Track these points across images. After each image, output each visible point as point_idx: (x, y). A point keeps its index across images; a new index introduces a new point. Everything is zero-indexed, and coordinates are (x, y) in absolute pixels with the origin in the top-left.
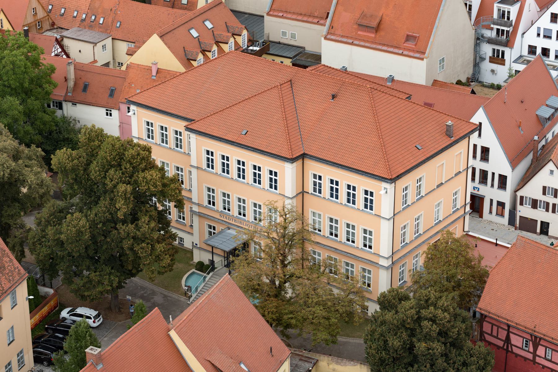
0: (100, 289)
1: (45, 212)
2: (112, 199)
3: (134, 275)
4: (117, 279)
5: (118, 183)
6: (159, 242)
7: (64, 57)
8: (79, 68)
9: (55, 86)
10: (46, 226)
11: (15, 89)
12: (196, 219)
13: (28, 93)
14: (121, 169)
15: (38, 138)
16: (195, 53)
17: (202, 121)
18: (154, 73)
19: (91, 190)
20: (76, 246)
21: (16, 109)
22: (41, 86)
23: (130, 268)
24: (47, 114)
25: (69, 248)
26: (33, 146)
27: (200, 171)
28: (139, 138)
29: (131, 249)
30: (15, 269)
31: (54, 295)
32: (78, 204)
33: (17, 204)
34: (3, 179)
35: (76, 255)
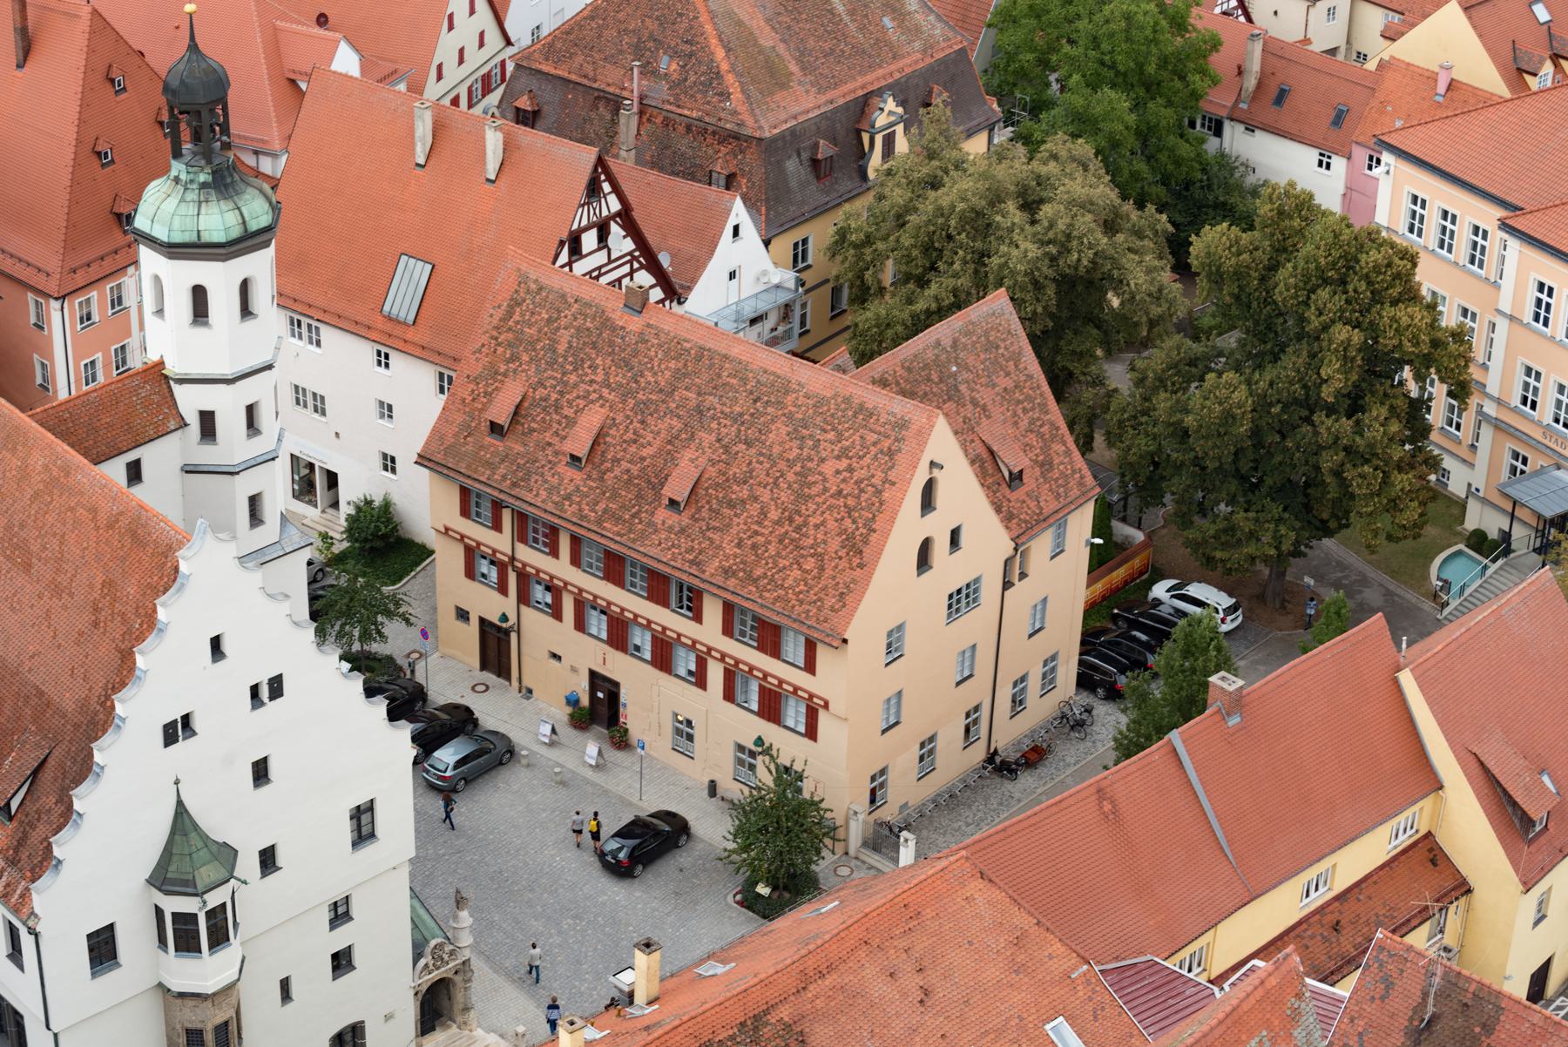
0: (1251, 549)
1: (1156, 358)
2: (1313, 356)
3: (1329, 533)
4: (1293, 535)
5: (1333, 322)
6: (1400, 470)
7: (1242, 19)
8: (1274, 49)
9: (1215, 82)
10: (1155, 390)
11: (1125, 75)
12: (1487, 433)
13: (1152, 87)
14: (1346, 292)
15: (1160, 190)
16: (1536, 59)
17: (1539, 214)
18: (1441, 89)
19: (1269, 328)
20: (1215, 446)
21: (1120, 119)
22: (1182, 78)
23: (1325, 516)
24: (1187, 141)
25: (1199, 446)
26: (1151, 208)
27: (1516, 327)
28: (1388, 229)
29: (1337, 474)
30: (1074, 472)
31: (1144, 546)
32: (1232, 353)
33: (1095, 331)
34: (1076, 269)
35: (1211, 465)
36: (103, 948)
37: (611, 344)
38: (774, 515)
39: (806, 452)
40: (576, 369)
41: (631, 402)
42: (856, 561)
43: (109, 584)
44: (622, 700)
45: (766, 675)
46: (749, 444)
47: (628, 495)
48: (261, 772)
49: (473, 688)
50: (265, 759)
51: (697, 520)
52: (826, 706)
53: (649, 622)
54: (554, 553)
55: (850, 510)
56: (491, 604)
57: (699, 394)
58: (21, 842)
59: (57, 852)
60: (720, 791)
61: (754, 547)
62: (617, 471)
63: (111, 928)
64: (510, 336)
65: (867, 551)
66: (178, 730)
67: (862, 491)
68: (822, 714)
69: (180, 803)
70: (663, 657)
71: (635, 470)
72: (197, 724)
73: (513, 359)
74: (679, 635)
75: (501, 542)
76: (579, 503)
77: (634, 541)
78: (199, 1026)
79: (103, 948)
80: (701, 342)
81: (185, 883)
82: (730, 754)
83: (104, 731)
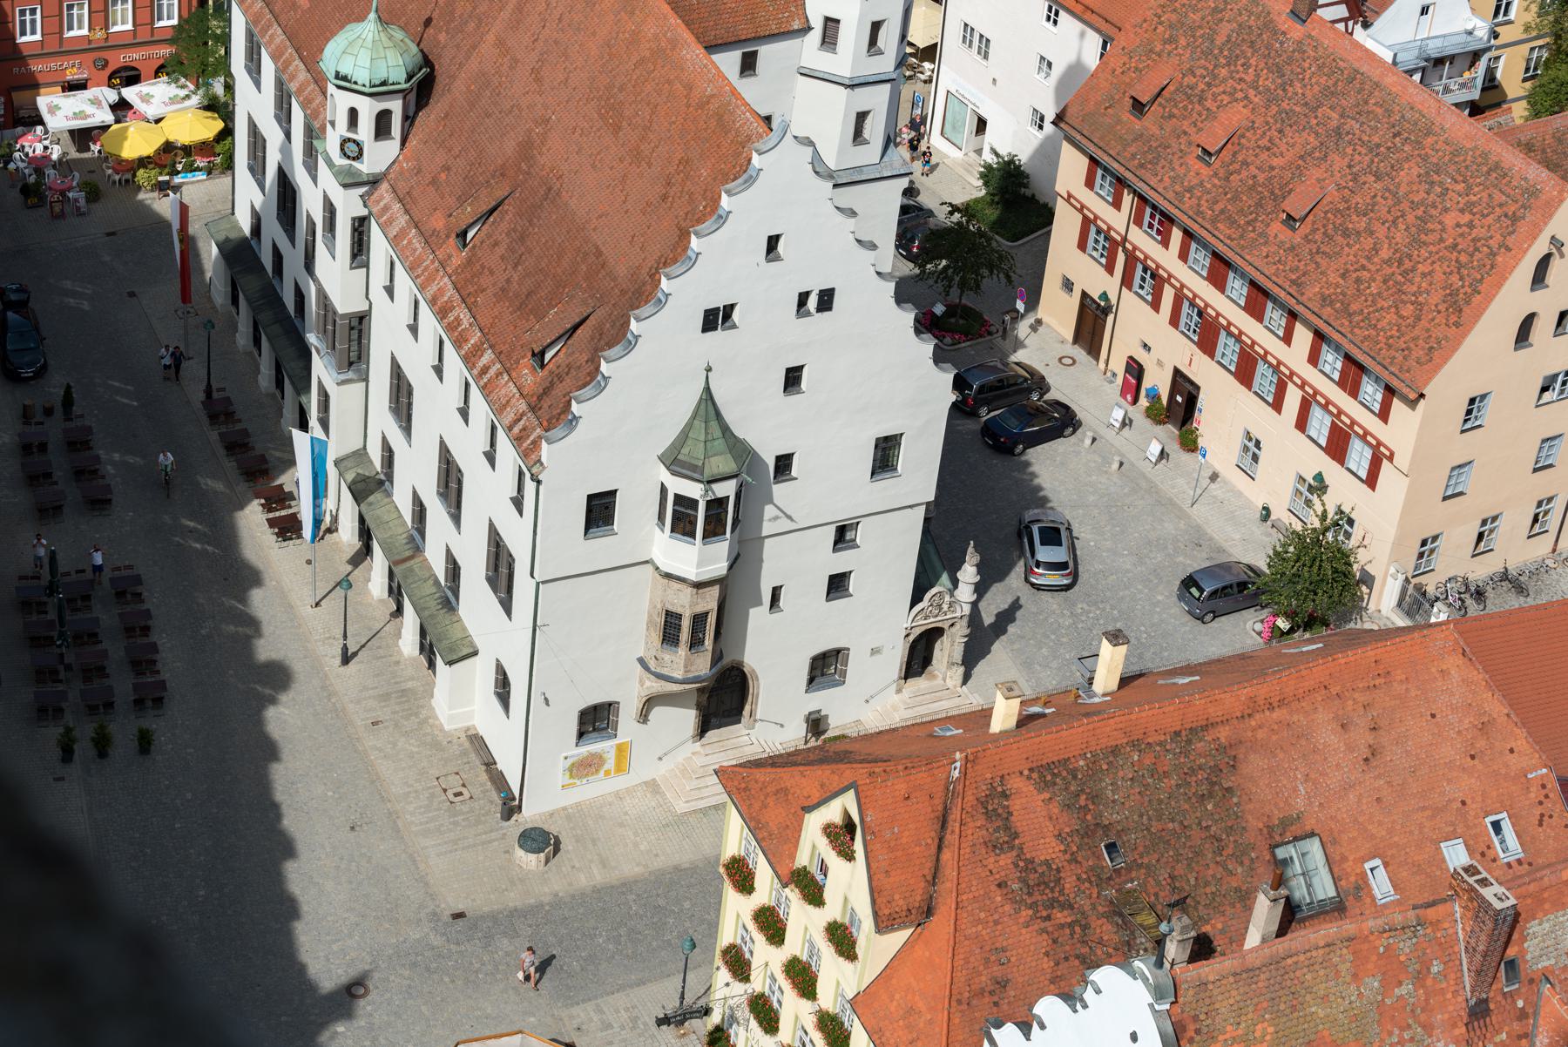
36: (600, 511)
37: (1269, 47)
38: (1385, 253)
39: (1432, 197)
40: (1229, 65)
41: (1275, 109)
42: (1453, 319)
43: (685, 162)
44: (1199, 405)
45: (1340, 412)
46: (1378, 178)
47: (1248, 201)
48: (793, 378)
49: (1060, 360)
50: (800, 369)
51: (1309, 241)
52: (1391, 458)
53: (1241, 332)
54: (1165, 243)
55: (1460, 266)
56: (1097, 280)
57: (1342, 116)
58: (546, 391)
59: (575, 408)
60: (1273, 517)
61: (1358, 281)
62: (1245, 174)
63: (612, 494)
64: (1174, 17)
65: (1467, 310)
66: (717, 318)
67: (1476, 249)
68: (1385, 462)
69: (707, 389)
70: (1245, 372)
71: (1261, 178)
72: (736, 316)
73: (1171, 40)
74: (1266, 353)
75: (1117, 220)
76: (1199, 199)
77: (1243, 248)
78: (679, 610)
79: (600, 511)
80: (1356, 65)
81: (694, 468)
82: (1290, 484)
83: (646, 302)
